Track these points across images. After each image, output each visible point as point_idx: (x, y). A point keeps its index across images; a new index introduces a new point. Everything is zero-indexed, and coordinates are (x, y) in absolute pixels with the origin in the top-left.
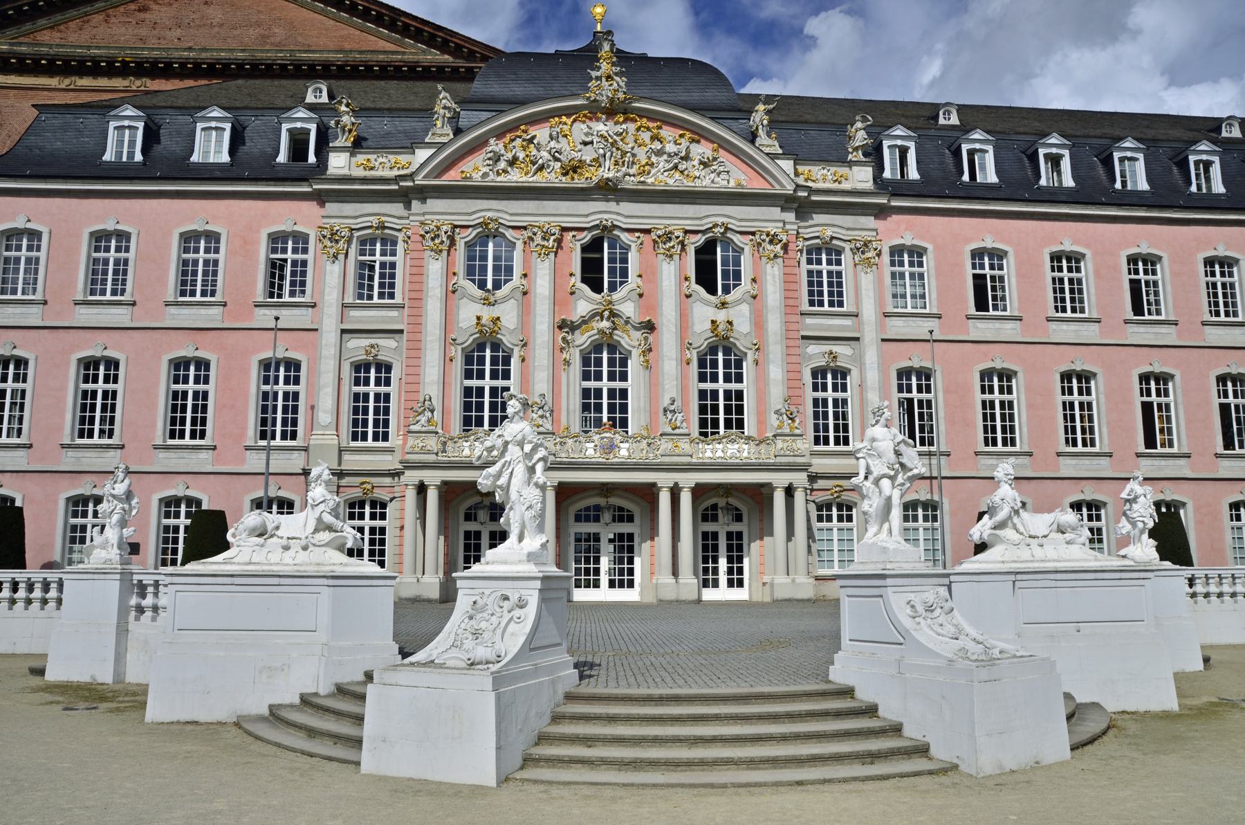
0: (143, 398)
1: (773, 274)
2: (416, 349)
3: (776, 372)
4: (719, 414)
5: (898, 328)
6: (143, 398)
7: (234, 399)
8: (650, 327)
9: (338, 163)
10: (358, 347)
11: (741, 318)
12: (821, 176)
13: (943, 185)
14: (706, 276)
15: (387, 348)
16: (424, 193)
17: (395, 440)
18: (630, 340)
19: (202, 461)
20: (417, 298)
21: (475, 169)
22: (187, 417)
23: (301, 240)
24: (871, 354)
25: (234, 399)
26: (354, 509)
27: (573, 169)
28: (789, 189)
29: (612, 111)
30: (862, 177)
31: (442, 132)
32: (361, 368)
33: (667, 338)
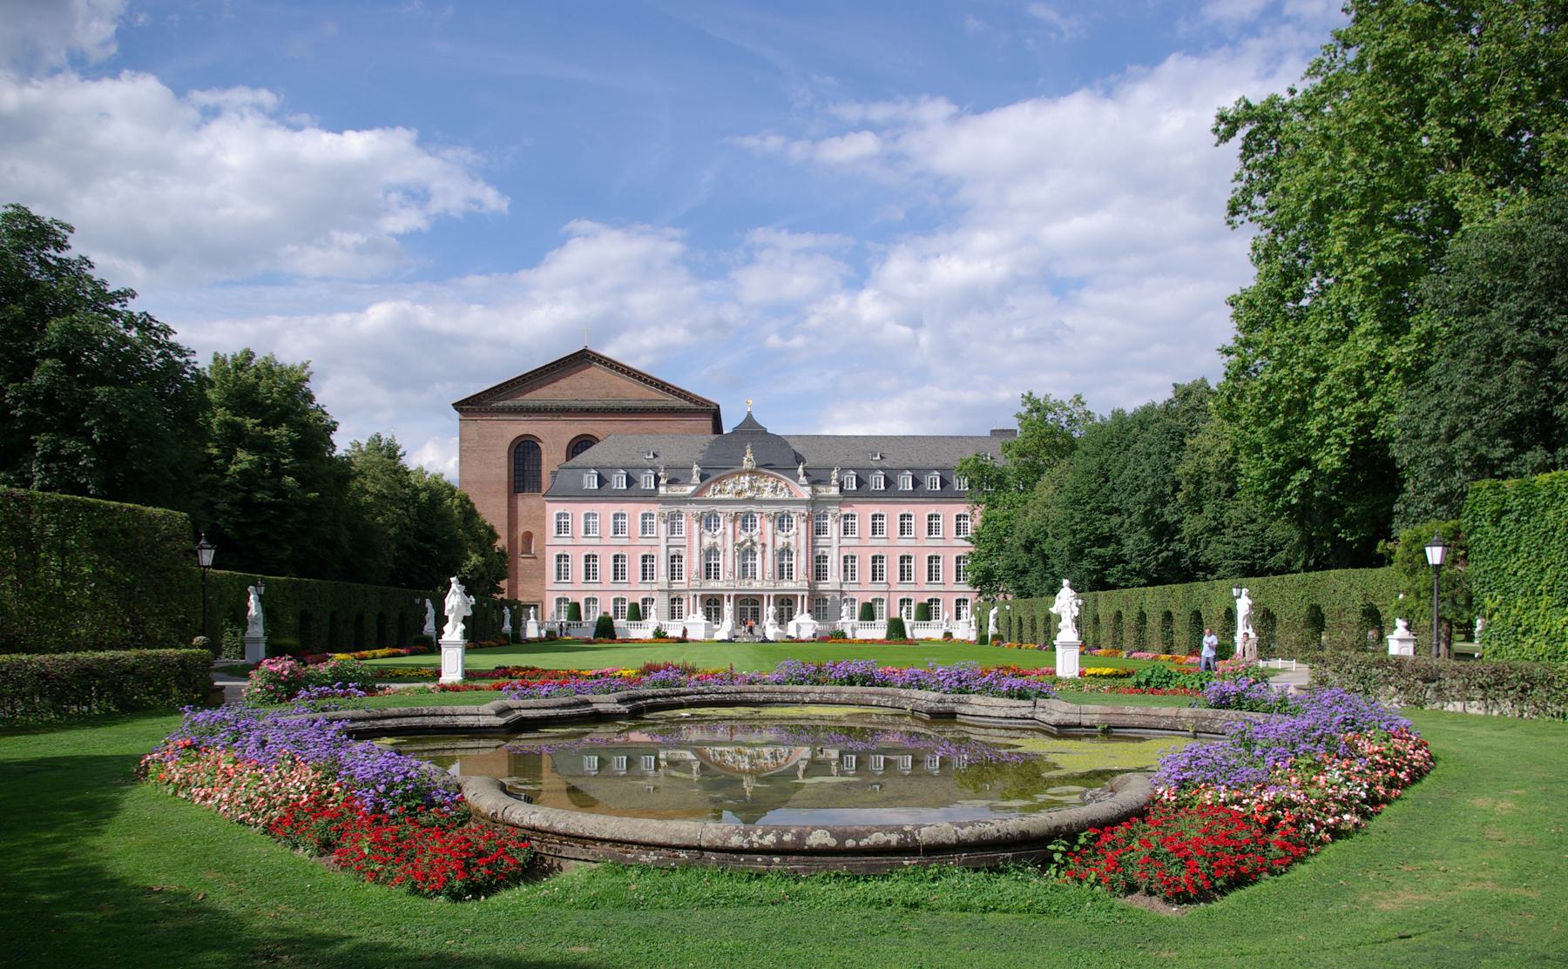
0: (605, 567)
1: (803, 526)
2: (690, 552)
3: (803, 558)
4: (783, 572)
5: (844, 542)
6: (605, 567)
7: (634, 567)
8: (764, 545)
9: (662, 490)
10: (673, 551)
11: (792, 540)
12: (823, 491)
13: (863, 491)
14: (781, 527)
15: (683, 551)
16: (691, 502)
17: (685, 580)
18: (758, 549)
19: (625, 587)
20: (690, 536)
21: (709, 495)
22: (618, 573)
23: (652, 516)
24: (835, 551)
25: (634, 567)
26: (673, 601)
27: (740, 493)
28: (807, 497)
29: (751, 472)
30: (834, 491)
31: (696, 479)
32: (673, 558)
33: (769, 549)
